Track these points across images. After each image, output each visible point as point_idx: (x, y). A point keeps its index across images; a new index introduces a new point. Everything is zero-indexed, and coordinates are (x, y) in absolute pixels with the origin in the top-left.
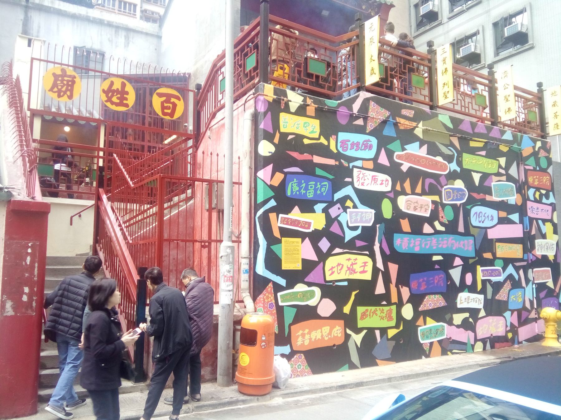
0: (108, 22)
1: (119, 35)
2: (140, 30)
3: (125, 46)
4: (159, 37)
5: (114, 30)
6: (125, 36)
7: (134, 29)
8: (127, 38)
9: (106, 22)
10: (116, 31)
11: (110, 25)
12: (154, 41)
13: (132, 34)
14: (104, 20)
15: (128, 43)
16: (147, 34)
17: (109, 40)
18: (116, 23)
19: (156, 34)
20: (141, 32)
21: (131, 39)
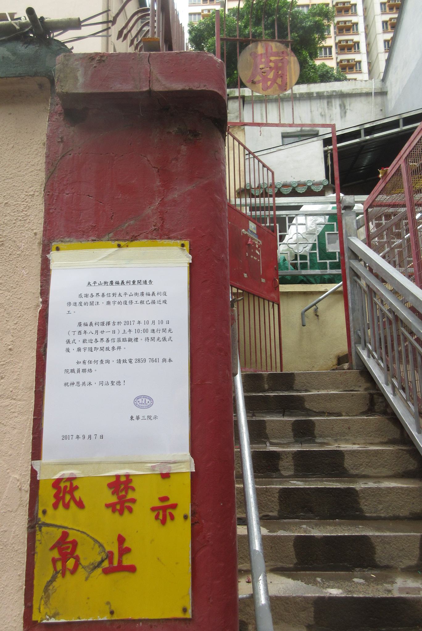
0: (318, 93)
1: (332, 106)
2: (359, 91)
3: (342, 117)
4: (382, 93)
5: (325, 101)
6: (340, 106)
7: (350, 92)
8: (343, 107)
9: (315, 95)
10: (328, 105)
11: (320, 96)
12: (379, 99)
13: (347, 101)
14: (312, 93)
15: (345, 113)
16: (368, 94)
17: (322, 115)
18: (327, 92)
19: (379, 91)
20: (360, 95)
21: (347, 107)
